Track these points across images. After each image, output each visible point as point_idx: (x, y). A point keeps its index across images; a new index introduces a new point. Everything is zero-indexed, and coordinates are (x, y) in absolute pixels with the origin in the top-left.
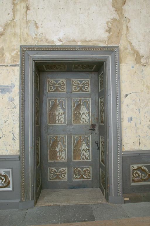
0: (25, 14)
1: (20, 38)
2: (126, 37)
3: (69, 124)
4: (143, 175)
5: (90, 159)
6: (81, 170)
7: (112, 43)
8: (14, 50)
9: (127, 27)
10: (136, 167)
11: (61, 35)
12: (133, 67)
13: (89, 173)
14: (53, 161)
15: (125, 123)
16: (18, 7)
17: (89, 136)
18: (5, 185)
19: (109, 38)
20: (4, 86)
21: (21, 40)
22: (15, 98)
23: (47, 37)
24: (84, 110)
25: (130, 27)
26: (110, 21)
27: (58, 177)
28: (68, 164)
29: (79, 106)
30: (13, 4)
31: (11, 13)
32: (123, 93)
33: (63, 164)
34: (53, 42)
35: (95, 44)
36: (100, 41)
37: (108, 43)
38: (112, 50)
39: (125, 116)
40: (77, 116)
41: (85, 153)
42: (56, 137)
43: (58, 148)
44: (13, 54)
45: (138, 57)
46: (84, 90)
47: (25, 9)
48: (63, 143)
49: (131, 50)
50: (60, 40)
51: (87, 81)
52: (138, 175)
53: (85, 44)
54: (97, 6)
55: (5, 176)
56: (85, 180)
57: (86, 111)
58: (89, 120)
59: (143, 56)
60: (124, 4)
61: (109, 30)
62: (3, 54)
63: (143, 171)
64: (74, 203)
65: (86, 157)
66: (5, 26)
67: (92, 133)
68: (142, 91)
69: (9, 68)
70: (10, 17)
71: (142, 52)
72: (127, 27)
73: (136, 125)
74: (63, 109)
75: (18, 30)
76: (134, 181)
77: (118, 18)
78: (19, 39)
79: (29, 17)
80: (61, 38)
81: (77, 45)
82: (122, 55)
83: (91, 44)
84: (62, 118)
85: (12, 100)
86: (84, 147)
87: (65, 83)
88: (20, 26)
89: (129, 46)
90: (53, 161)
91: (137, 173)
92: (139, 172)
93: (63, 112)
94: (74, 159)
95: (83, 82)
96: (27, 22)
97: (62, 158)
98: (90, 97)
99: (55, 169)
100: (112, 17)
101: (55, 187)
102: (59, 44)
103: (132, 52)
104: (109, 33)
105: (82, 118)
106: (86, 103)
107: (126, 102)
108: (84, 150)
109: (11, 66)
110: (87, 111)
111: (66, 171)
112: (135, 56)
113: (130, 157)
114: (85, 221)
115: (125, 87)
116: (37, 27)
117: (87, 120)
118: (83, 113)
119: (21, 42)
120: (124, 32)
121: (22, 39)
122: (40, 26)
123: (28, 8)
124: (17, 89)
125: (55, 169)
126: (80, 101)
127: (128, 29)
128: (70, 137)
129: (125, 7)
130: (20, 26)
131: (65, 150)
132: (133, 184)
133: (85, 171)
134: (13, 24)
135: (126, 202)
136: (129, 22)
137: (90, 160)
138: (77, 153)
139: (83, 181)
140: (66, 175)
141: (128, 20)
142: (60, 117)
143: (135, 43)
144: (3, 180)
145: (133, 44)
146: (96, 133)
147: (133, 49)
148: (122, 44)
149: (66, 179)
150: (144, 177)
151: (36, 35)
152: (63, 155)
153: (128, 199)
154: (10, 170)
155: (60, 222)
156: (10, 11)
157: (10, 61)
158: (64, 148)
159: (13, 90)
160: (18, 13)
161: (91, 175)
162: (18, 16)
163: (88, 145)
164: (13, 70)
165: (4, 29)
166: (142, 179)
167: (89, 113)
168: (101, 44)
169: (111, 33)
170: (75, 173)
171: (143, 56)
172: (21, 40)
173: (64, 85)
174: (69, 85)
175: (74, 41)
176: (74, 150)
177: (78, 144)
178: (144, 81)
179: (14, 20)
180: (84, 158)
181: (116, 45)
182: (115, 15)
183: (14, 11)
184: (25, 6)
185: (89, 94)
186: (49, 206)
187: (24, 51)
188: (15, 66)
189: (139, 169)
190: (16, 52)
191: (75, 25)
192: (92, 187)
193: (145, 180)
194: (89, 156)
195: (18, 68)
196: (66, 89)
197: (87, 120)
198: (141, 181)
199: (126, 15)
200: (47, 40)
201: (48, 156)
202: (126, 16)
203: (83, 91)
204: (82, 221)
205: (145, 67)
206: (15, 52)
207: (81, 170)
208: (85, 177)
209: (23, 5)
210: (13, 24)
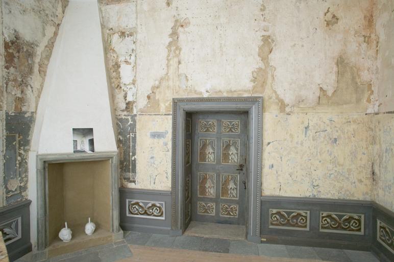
0: (177, 68)
1: (173, 90)
2: (271, 86)
3: (219, 162)
4: (282, 220)
5: (237, 197)
6: (228, 207)
7: (256, 92)
8: (168, 101)
9: (273, 76)
10: (275, 211)
11: (208, 87)
12: (277, 116)
13: (236, 210)
14: (202, 196)
15: (266, 170)
16: (171, 62)
17: (237, 176)
18: (160, 214)
19: (254, 87)
20: (159, 132)
21: (173, 92)
22: (168, 143)
23: (196, 88)
24: (233, 150)
25: (276, 76)
26: (256, 70)
27: (206, 212)
28: (216, 200)
29: (228, 147)
30: (167, 60)
31: (166, 68)
32: (266, 141)
33: (211, 200)
34: (201, 93)
35: (240, 94)
36: (245, 91)
37: (253, 93)
38: (254, 100)
39: (267, 162)
40: (226, 156)
41: (232, 191)
42: (206, 175)
43: (207, 185)
44: (167, 105)
45: (282, 106)
46: (234, 131)
47: (178, 63)
48: (212, 180)
49: (276, 98)
50: (207, 91)
51: (237, 122)
52: (277, 219)
53: (230, 95)
54: (243, 56)
55: (159, 207)
56: (232, 216)
57: (235, 151)
58: (238, 160)
59: (288, 105)
60: (271, 52)
61: (254, 80)
62: (159, 105)
63: (282, 216)
64: (216, 236)
65: (233, 196)
66: (161, 79)
67: (239, 173)
68: (285, 140)
69: (163, 117)
70: (164, 72)
71: (287, 101)
72: (273, 76)
73: (277, 172)
74: (213, 148)
75: (171, 83)
76: (272, 224)
77: (263, 67)
78: (172, 91)
79: (181, 71)
80: (208, 90)
81: (223, 96)
82: (266, 104)
83: (235, 95)
84: (212, 157)
85: (166, 144)
86: (231, 185)
87: (215, 124)
88: (173, 80)
89: (274, 95)
90: (202, 196)
91: (275, 217)
92: (278, 217)
93: (213, 151)
94: (222, 196)
95: (233, 123)
96: (178, 75)
97: (211, 194)
98: (239, 138)
99: (204, 204)
100: (258, 67)
101: (203, 220)
102: (206, 95)
103: (277, 101)
104: (254, 83)
105: (230, 158)
106: (235, 144)
107: (267, 150)
108: (231, 188)
109: (165, 115)
110: (236, 152)
111: (214, 207)
112: (280, 104)
113: (269, 202)
114: (220, 252)
115: (268, 136)
116: (187, 80)
117: (236, 160)
118: (232, 154)
119: (173, 94)
120: (269, 81)
121: (174, 91)
122: (189, 79)
123: (179, 63)
124: (170, 136)
125: (204, 204)
126: (230, 142)
127: (274, 78)
128: (218, 176)
129: (271, 56)
130: (173, 80)
131: (214, 187)
132: (271, 227)
133: (232, 208)
134: (167, 78)
135: (262, 242)
136: (275, 70)
137: (237, 199)
138: (225, 191)
139: (230, 218)
140: (214, 210)
141: (274, 69)
142: (210, 156)
143: (280, 92)
144: (158, 210)
145: (279, 93)
146: (244, 174)
147: (277, 98)
148: (267, 93)
149: (213, 214)
150: (282, 221)
151: (187, 87)
152: (212, 192)
153: (265, 240)
154: (164, 203)
155: (200, 250)
156: (164, 66)
157: (164, 111)
158: (212, 185)
159: (167, 136)
160: (172, 67)
161: (237, 212)
162: (171, 71)
163: (236, 184)
164: (167, 119)
165: (160, 83)
166: (281, 224)
167: (237, 154)
168: (246, 95)
169: (256, 83)
170: (222, 209)
171: (288, 105)
172: (173, 92)
173: (215, 126)
174: (220, 126)
175: (220, 91)
176: (222, 188)
177: (226, 183)
178: (287, 130)
179: (169, 74)
180: (232, 196)
181: (261, 95)
182: (261, 65)
183: (168, 66)
184: (177, 61)
185: (238, 135)
186: (194, 236)
187: (176, 103)
188: (169, 115)
189: (278, 213)
190: (169, 103)
191: (222, 76)
192: (238, 224)
193: (283, 225)
194: (236, 194)
195: (171, 117)
196: (216, 130)
197: (236, 160)
198: (280, 225)
199: (272, 63)
200: (195, 91)
201: (198, 192)
202: (272, 64)
203: (232, 132)
204: (218, 252)
205: (290, 116)
206: (169, 102)
207: (228, 207)
208: (232, 214)
209: (176, 60)
210: (167, 78)
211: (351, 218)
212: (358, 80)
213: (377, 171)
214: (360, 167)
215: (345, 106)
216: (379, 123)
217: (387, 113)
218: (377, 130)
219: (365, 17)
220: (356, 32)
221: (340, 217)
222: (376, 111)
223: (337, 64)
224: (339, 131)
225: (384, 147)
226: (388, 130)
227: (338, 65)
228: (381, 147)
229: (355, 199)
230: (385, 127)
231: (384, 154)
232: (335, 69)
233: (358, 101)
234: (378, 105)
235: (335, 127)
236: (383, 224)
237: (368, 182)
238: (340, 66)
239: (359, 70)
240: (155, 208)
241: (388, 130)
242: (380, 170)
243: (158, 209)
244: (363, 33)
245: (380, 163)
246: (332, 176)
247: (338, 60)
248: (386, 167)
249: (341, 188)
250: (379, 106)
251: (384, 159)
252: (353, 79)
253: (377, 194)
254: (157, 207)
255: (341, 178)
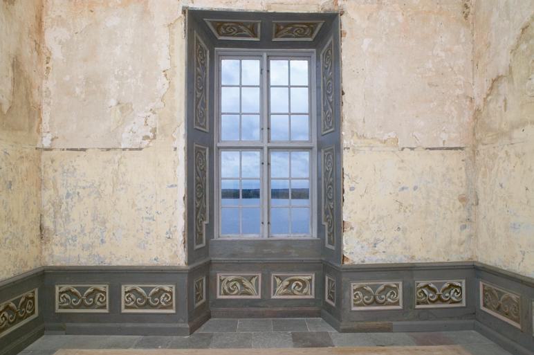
211: (27, 298)
212: (31, 100)
213: (48, 223)
214: (31, 222)
215: (19, 133)
216: (52, 162)
217: (67, 149)
218: (50, 171)
219: (36, 16)
220: (30, 33)
221: (16, 302)
222: (46, 143)
223: (13, 66)
224: (14, 170)
225: (63, 192)
226: (72, 169)
227: (13, 70)
228: (57, 191)
229: (28, 269)
230: (66, 168)
231: (64, 201)
232: (11, 74)
233: (31, 128)
234: (50, 138)
235: (10, 164)
236: (65, 287)
237: (37, 241)
238: (15, 71)
239: (31, 84)
240: (163, 296)
241: (72, 169)
242: (54, 222)
243: (168, 295)
244: (36, 39)
245: (55, 213)
246: (8, 241)
247: (14, 61)
248: (68, 216)
249: (16, 257)
250: (52, 140)
251: (64, 207)
252: (27, 96)
253: (51, 255)
254: (166, 292)
255: (16, 243)
